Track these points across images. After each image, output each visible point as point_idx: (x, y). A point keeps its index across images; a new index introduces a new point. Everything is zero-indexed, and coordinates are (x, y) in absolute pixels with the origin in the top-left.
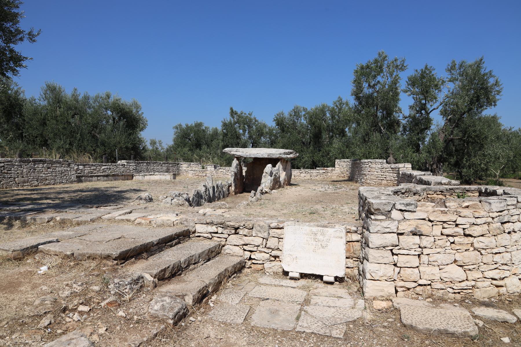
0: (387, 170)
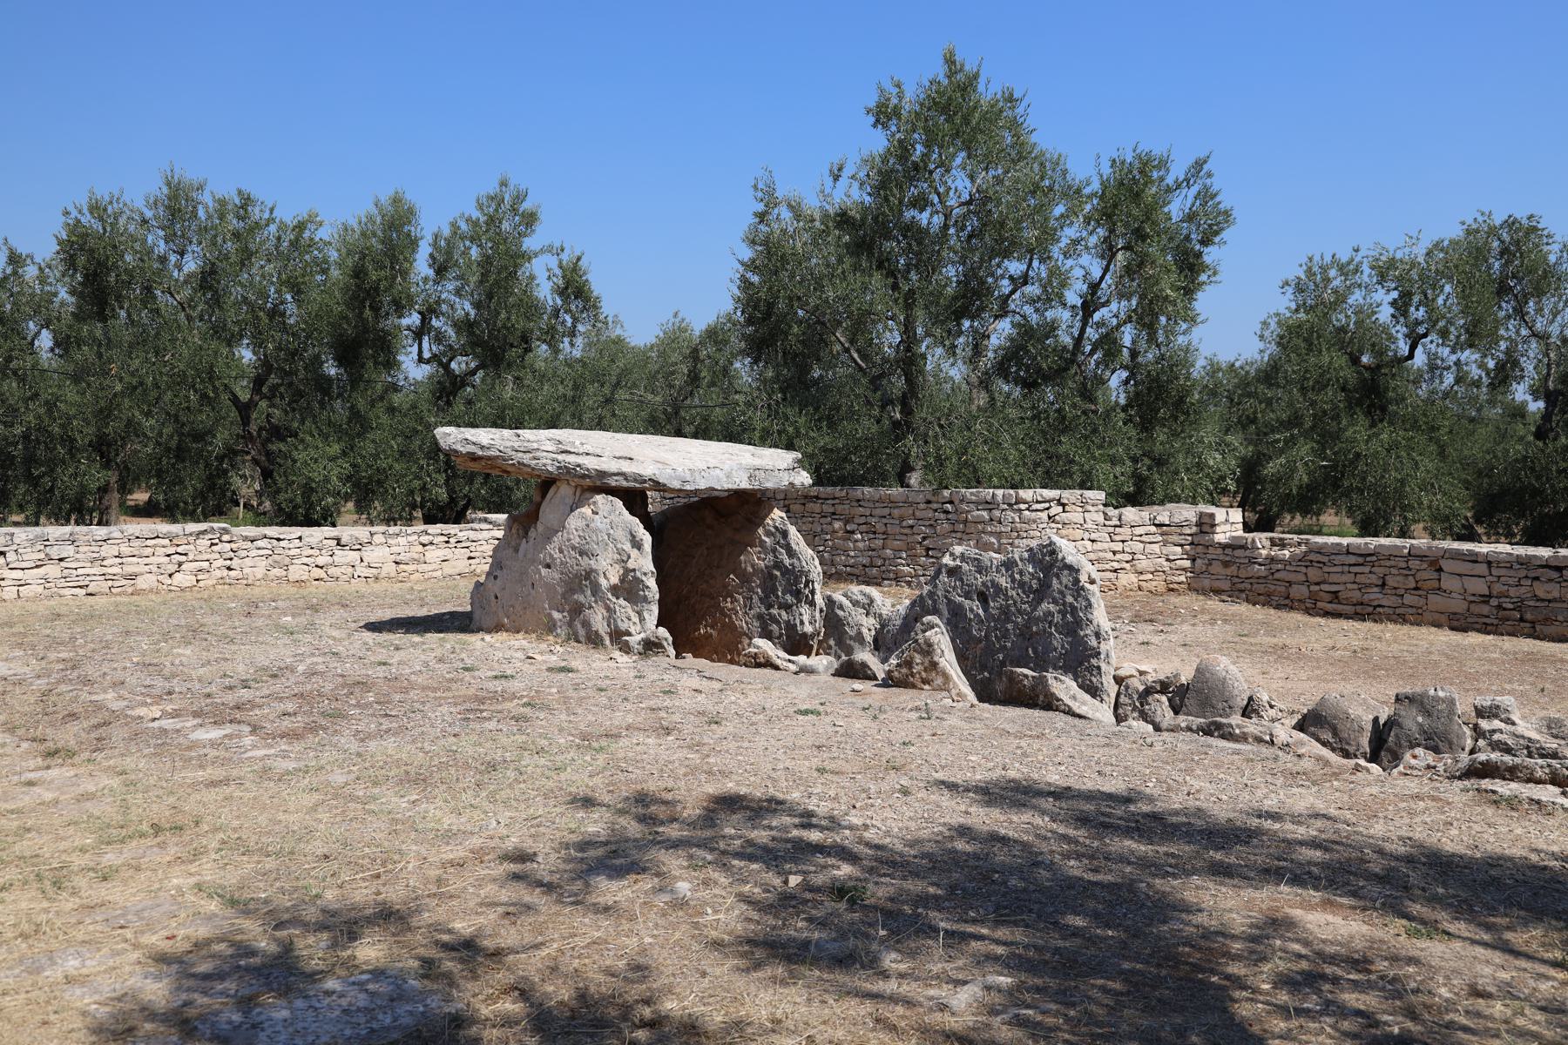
0: (1138, 531)
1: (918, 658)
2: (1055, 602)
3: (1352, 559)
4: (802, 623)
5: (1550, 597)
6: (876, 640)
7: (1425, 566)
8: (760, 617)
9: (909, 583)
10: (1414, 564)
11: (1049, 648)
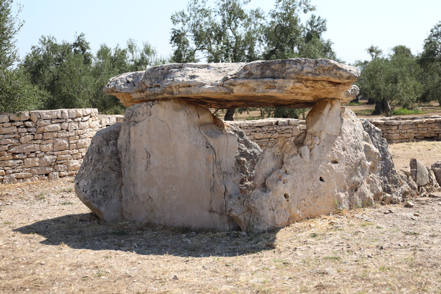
5: (260, 138)
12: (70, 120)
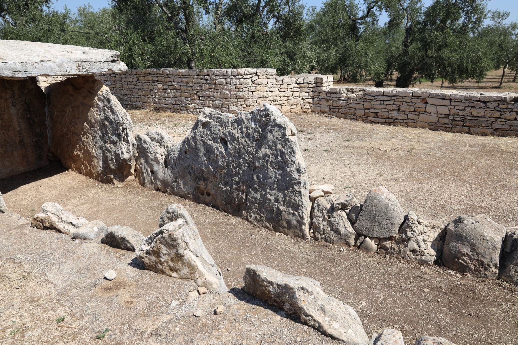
0: (290, 86)
1: (164, 250)
2: (270, 148)
3: (385, 98)
4: (122, 153)
5: (479, 115)
6: (165, 162)
7: (419, 101)
8: (101, 147)
9: (192, 112)
10: (414, 100)
11: (266, 177)
12: (232, 77)
